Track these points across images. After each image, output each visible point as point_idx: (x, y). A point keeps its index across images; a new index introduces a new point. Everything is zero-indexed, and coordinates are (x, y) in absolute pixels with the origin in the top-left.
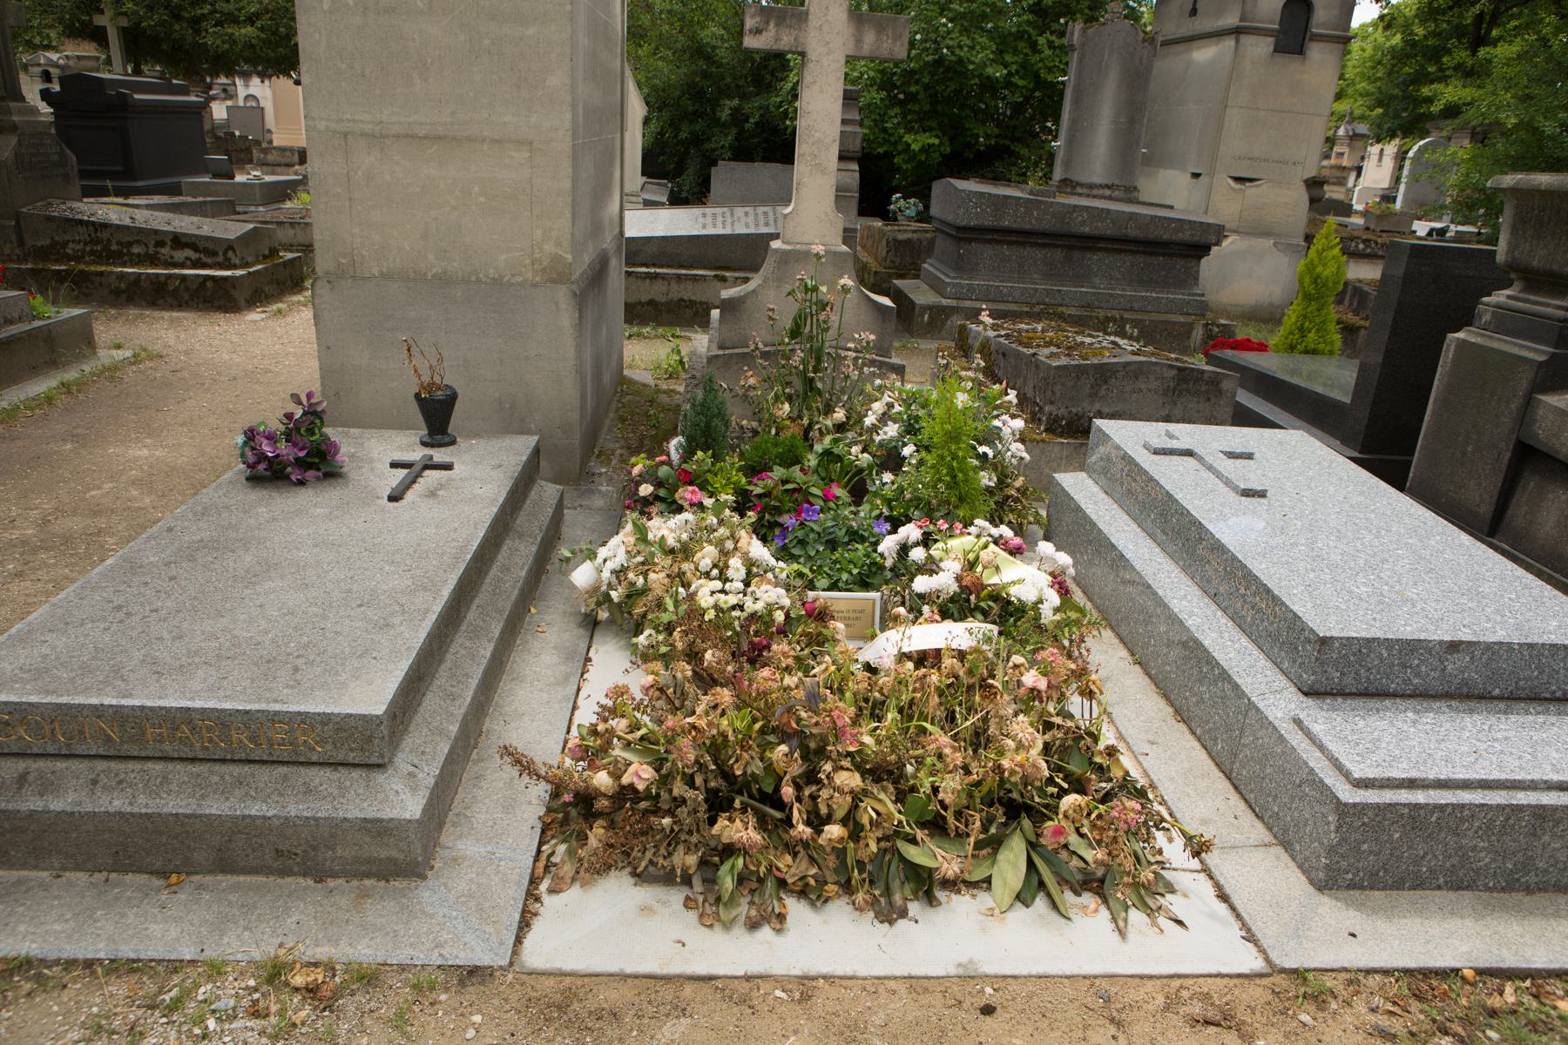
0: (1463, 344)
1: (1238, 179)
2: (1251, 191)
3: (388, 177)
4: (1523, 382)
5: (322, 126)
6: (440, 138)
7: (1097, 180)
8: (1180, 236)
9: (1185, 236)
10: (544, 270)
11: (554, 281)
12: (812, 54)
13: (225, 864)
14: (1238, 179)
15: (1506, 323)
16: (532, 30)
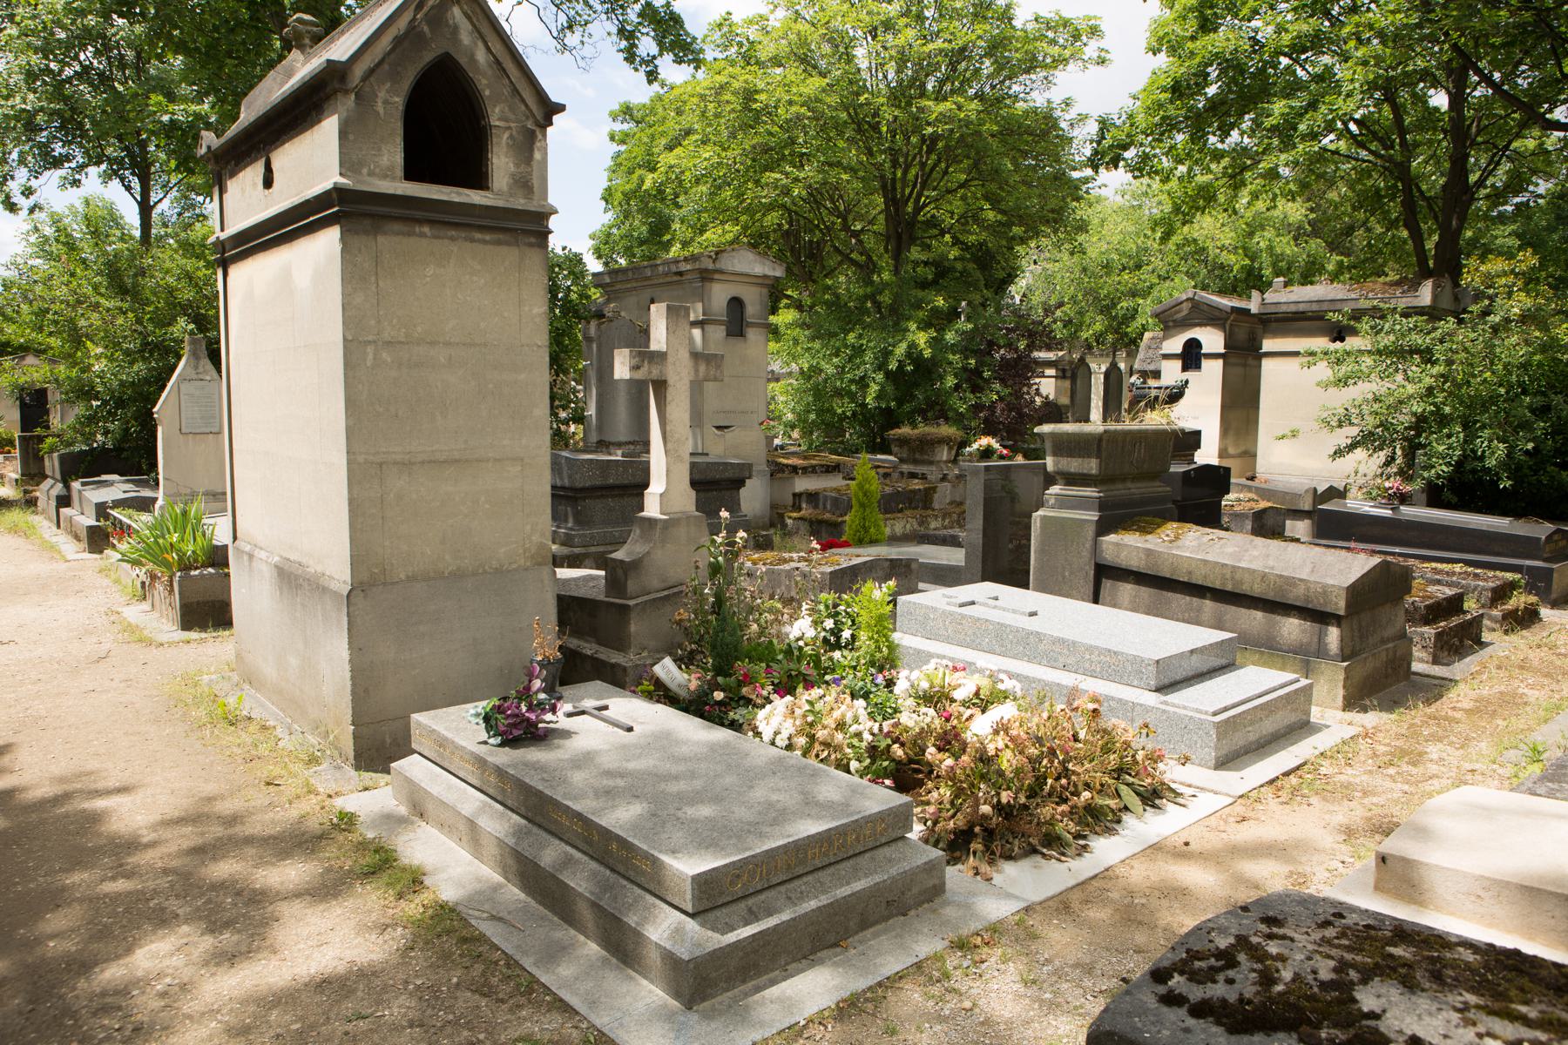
0: (1044, 518)
1: (718, 428)
2: (728, 435)
3: (414, 496)
4: (1090, 532)
5: (361, 459)
6: (457, 461)
7: (623, 439)
8: (727, 475)
9: (729, 474)
10: (532, 557)
11: (540, 564)
12: (671, 382)
13: (864, 925)
14: (718, 428)
15: (1063, 503)
16: (522, 376)
